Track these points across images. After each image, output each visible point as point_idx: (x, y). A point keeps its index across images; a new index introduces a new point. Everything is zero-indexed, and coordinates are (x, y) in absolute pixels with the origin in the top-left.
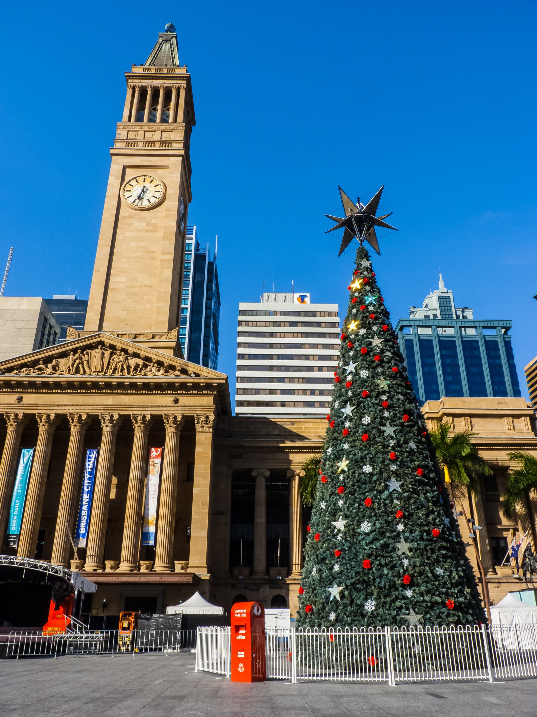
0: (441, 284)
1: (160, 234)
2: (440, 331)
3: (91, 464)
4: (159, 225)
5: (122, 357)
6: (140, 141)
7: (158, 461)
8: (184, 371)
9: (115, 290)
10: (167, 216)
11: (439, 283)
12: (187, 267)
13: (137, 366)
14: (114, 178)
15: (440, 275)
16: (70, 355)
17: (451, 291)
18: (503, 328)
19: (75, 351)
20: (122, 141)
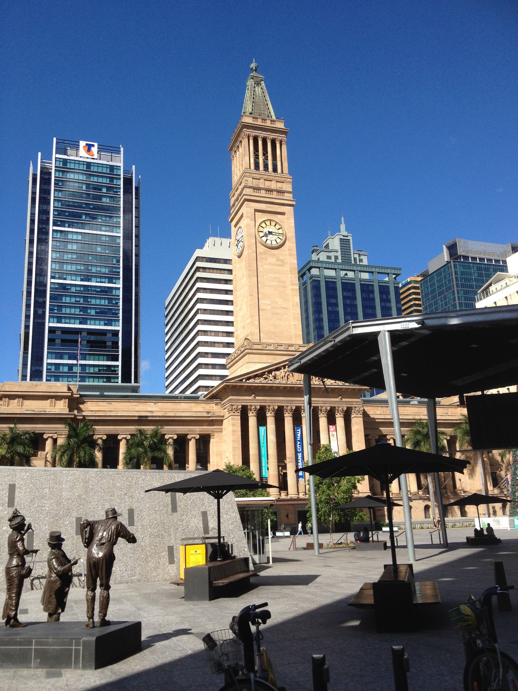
0: (343, 227)
1: (287, 268)
2: (343, 273)
3: (299, 435)
4: (285, 261)
6: (263, 189)
7: (335, 433)
9: (264, 310)
10: (290, 255)
11: (341, 225)
12: (117, 192)
14: (250, 220)
15: (343, 218)
16: (281, 369)
17: (351, 235)
18: (394, 274)
20: (250, 187)
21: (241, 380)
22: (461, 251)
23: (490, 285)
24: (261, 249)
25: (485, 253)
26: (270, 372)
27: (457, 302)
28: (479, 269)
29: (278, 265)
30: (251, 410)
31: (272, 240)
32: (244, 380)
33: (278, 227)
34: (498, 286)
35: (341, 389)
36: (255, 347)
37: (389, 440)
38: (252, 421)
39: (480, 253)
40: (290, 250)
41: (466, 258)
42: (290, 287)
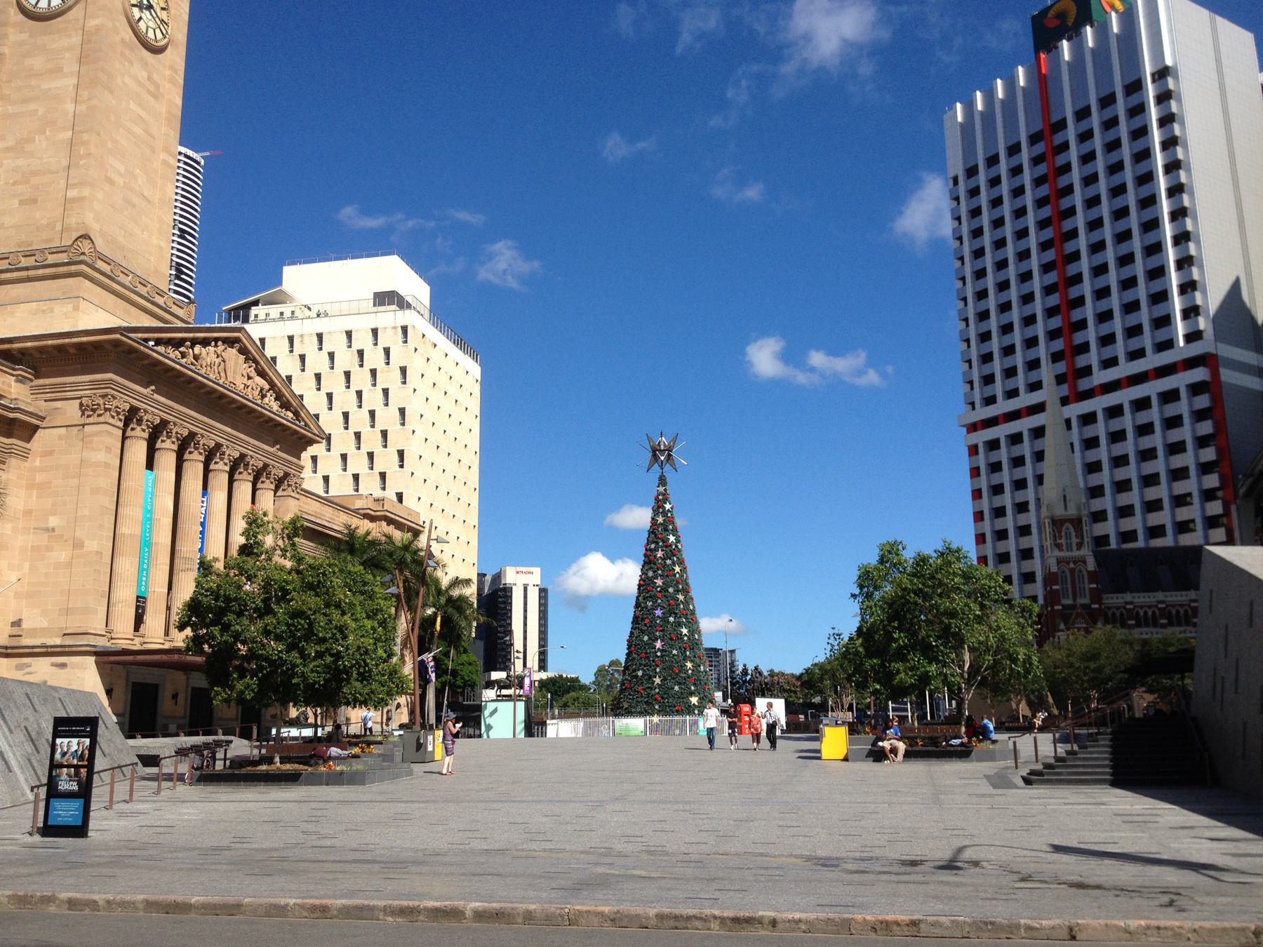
1: (163, 109)
5: (253, 374)
10: (172, 81)
19: (216, 340)
21: (146, 340)
23: (256, 303)
26: (194, 342)
29: (149, 92)
32: (151, 343)
34: (274, 311)
38: (138, 450)
40: (172, 68)
42: (163, 156)
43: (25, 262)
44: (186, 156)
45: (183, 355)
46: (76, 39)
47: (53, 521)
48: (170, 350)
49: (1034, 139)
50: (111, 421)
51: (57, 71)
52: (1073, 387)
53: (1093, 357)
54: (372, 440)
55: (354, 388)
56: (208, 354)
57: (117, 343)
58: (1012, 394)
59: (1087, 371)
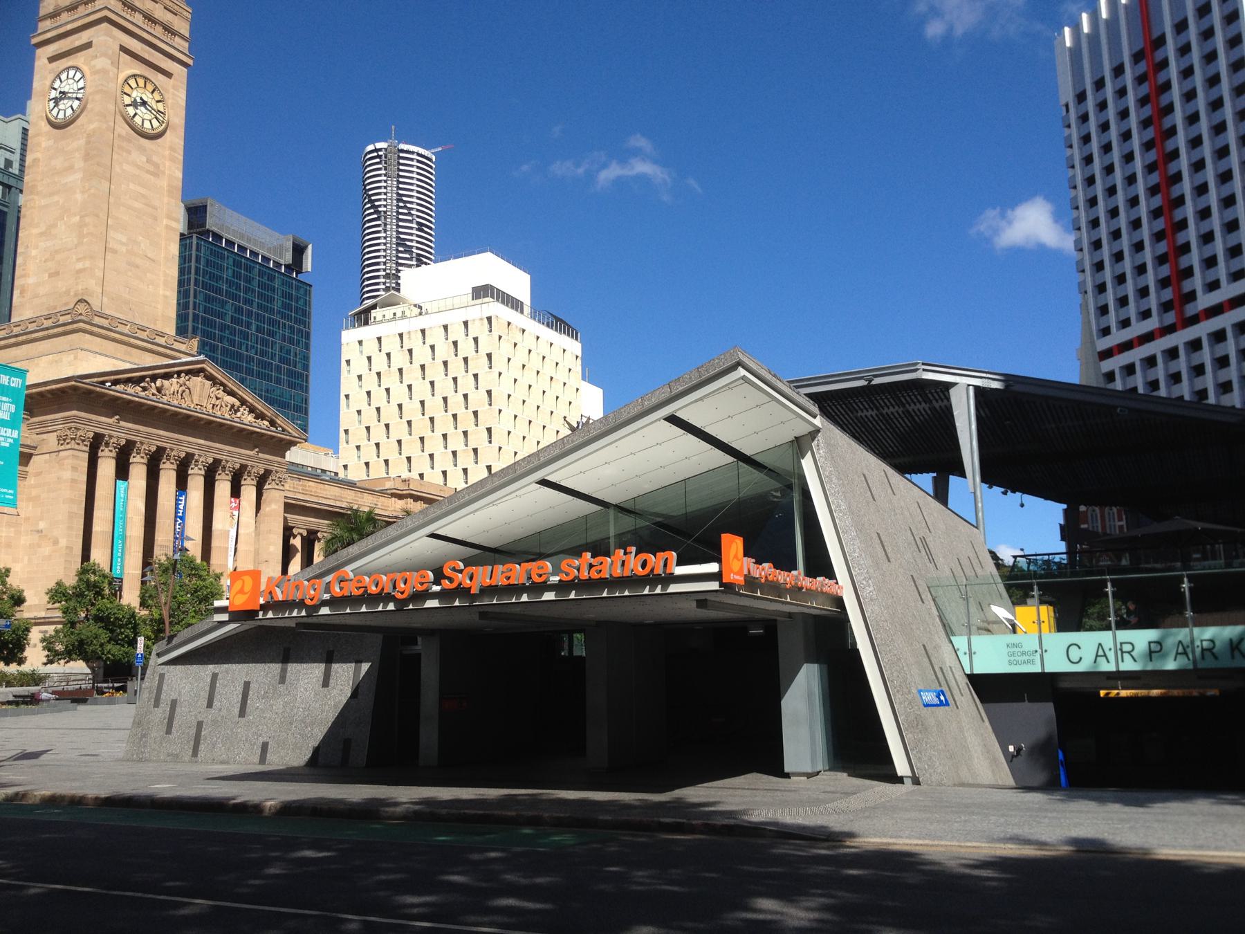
1: (164, 183)
5: (221, 393)
8: (273, 423)
9: (115, 252)
10: (172, 159)
13: (233, 406)
19: (179, 373)
21: (103, 383)
22: (211, 224)
23: (374, 307)
24: (124, 129)
25: (249, 240)
26: (154, 378)
27: (191, 311)
28: (237, 264)
29: (148, 172)
30: (107, 445)
31: (143, 118)
32: (108, 384)
33: (157, 96)
34: (388, 312)
35: (263, 435)
36: (97, 320)
37: (295, 537)
38: (107, 467)
39: (242, 237)
40: (172, 149)
41: (218, 237)
42: (165, 222)
43: (47, 323)
44: (419, 155)
45: (144, 389)
46: (82, 142)
47: (42, 525)
48: (130, 389)
49: (1137, 57)
50: (77, 447)
51: (70, 169)
52: (1181, 312)
53: (1197, 282)
54: (466, 421)
55: (451, 375)
56: (172, 385)
57: (75, 388)
58: (1125, 323)
59: (1192, 296)
